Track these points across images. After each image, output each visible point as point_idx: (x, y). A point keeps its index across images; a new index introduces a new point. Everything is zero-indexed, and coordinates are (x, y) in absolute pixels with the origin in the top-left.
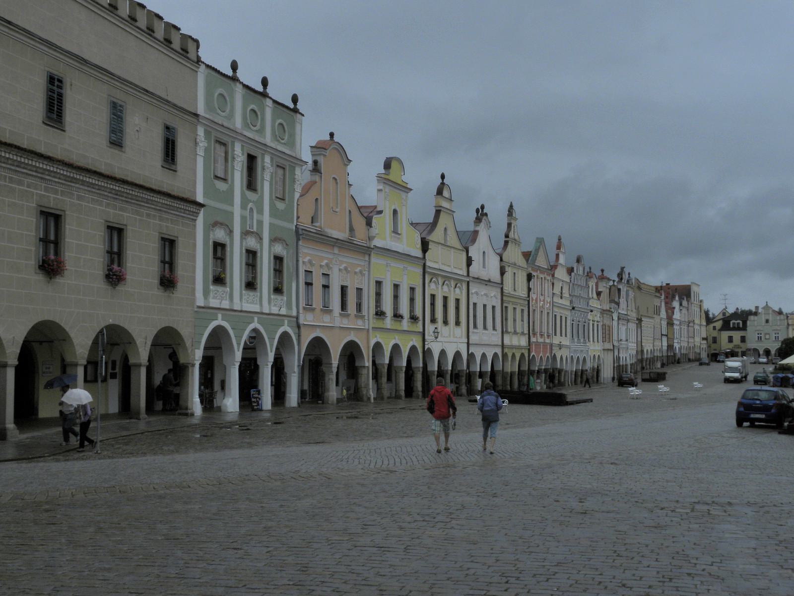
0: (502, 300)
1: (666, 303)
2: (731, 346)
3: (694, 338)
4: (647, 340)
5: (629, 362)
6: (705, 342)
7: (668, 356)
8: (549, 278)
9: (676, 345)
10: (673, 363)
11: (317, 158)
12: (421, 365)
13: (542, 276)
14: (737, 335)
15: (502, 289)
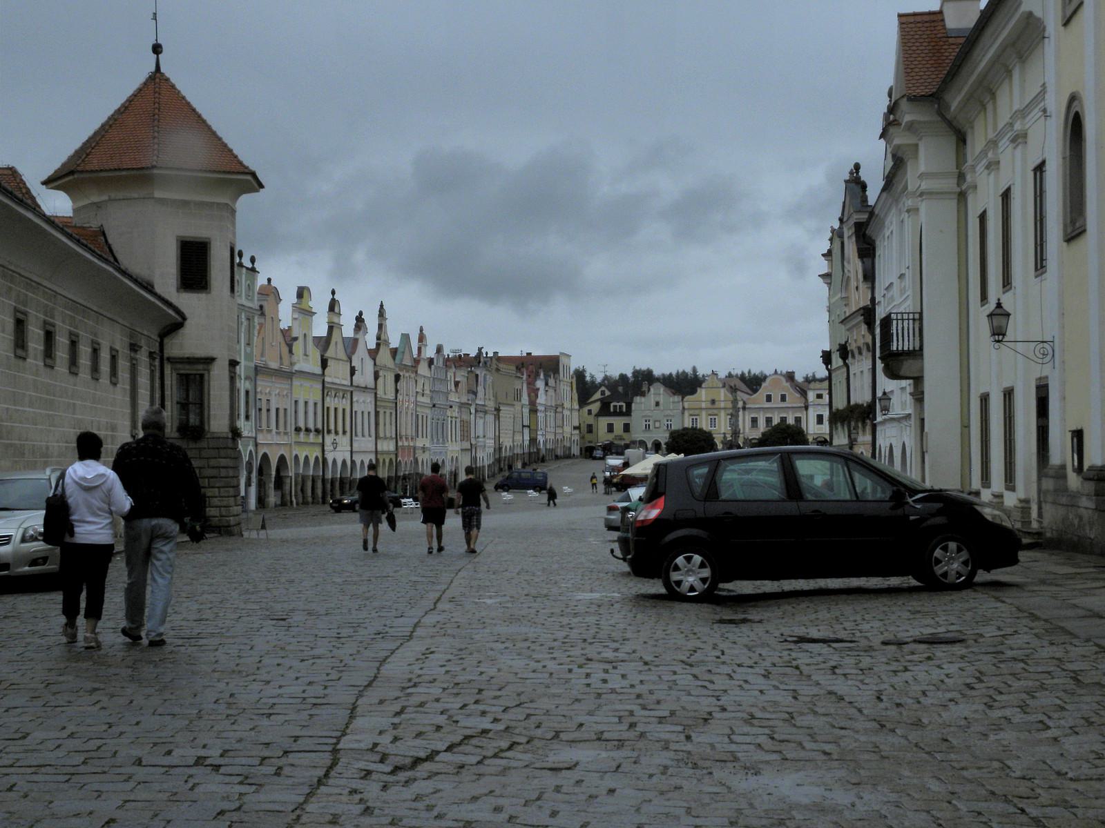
0: (376, 405)
1: (529, 384)
2: (610, 437)
3: (562, 427)
4: (506, 434)
5: (486, 463)
6: (577, 432)
7: (530, 454)
8: (413, 375)
9: (541, 439)
10: (535, 462)
11: (262, 303)
12: (321, 474)
13: (407, 375)
14: (618, 423)
15: (376, 394)
